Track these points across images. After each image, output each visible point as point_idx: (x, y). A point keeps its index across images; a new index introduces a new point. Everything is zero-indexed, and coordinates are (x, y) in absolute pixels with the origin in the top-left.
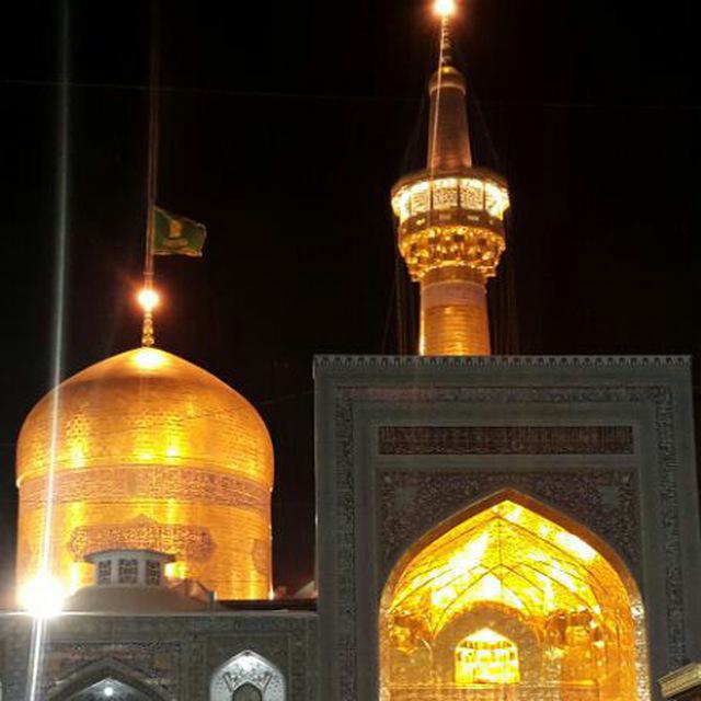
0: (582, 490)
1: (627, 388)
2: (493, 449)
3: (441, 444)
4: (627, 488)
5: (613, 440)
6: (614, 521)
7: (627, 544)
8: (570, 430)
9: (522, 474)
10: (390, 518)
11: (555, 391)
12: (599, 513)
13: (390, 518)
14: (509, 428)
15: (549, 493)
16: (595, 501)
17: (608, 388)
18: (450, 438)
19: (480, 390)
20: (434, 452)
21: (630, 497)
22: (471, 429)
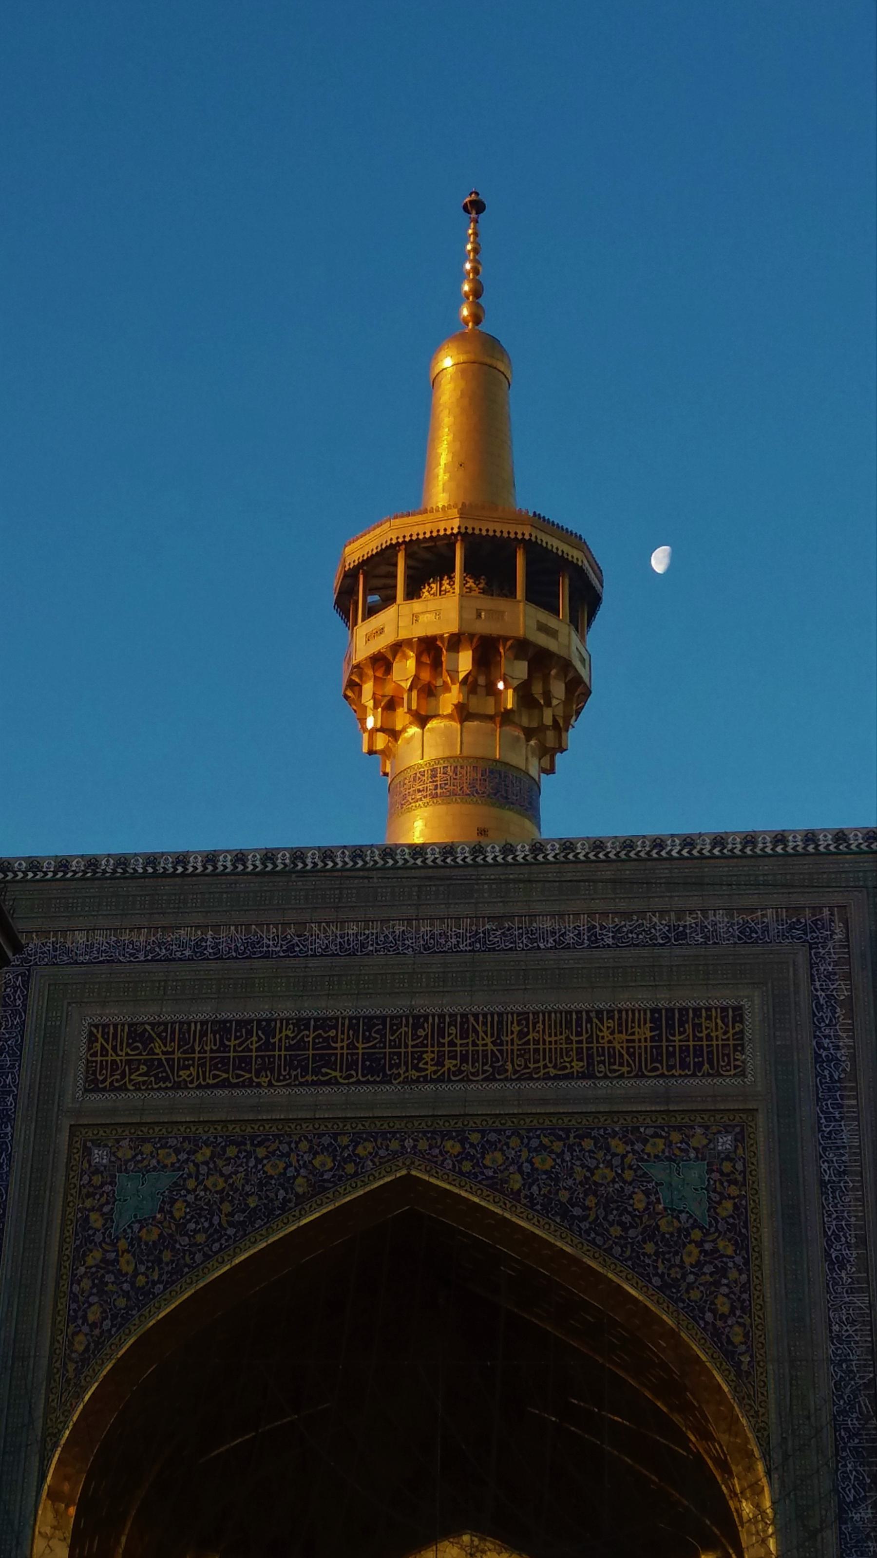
0: (604, 1173)
1: (729, 912)
2: (376, 1069)
3: (244, 1063)
4: (727, 1167)
5: (683, 1042)
6: (691, 1255)
7: (723, 1317)
8: (572, 1021)
9: (446, 1135)
10: (94, 1257)
11: (548, 925)
12: (651, 1233)
13: (94, 1257)
14: (419, 1021)
15: (516, 1181)
16: (639, 1202)
17: (680, 914)
18: (268, 1046)
19: (353, 929)
20: (225, 1084)
21: (733, 1190)
22: (324, 1023)
